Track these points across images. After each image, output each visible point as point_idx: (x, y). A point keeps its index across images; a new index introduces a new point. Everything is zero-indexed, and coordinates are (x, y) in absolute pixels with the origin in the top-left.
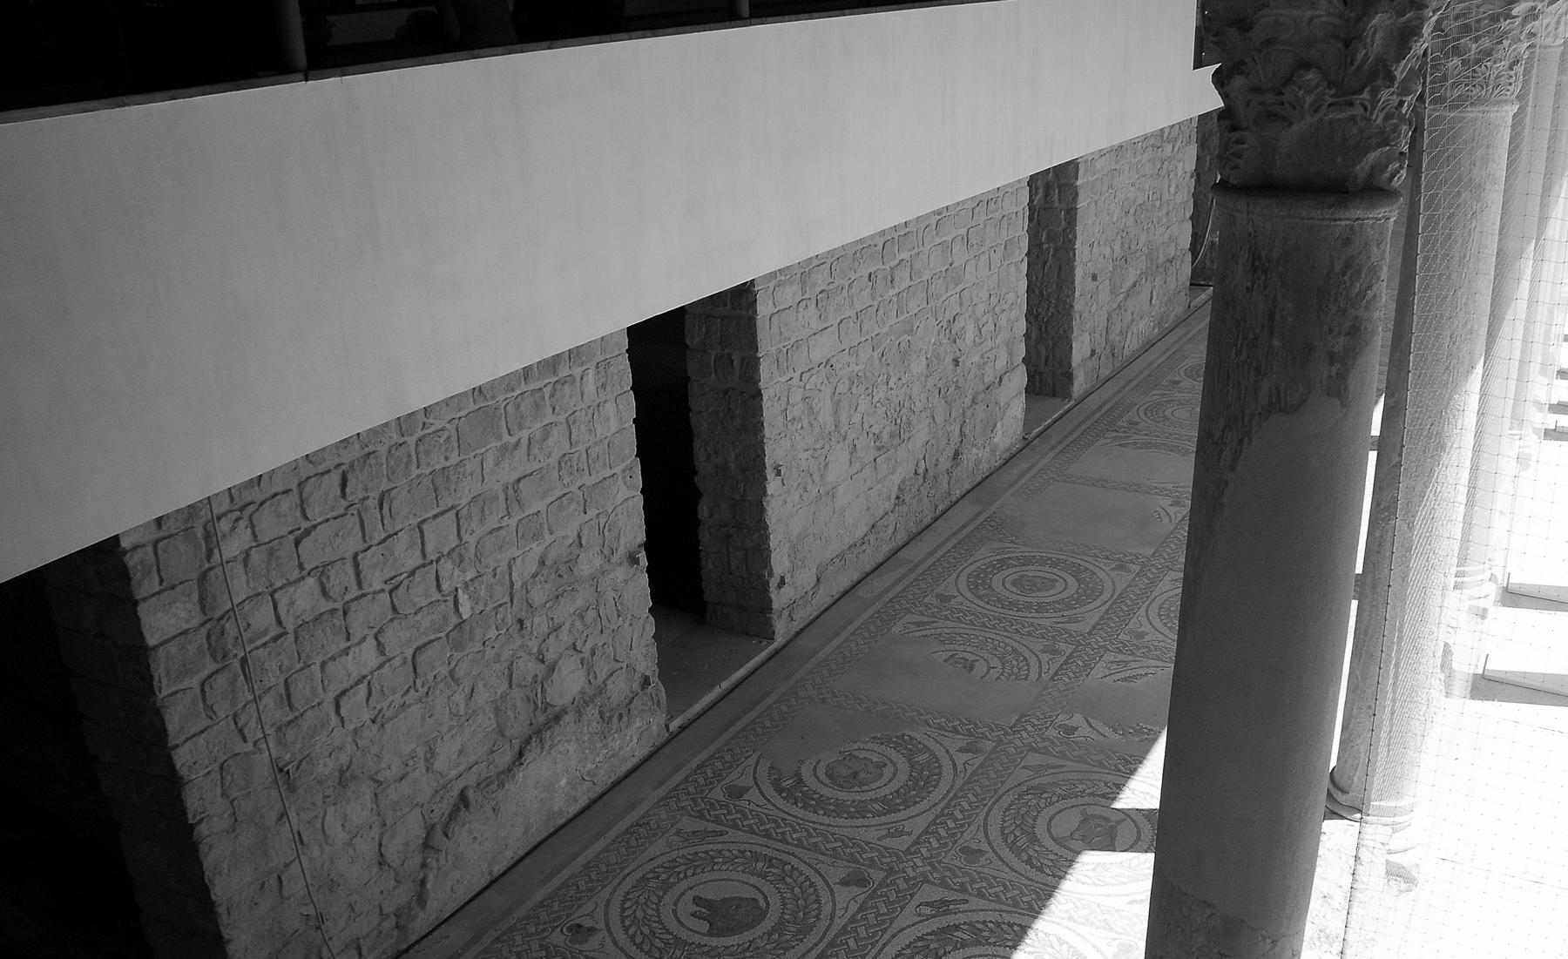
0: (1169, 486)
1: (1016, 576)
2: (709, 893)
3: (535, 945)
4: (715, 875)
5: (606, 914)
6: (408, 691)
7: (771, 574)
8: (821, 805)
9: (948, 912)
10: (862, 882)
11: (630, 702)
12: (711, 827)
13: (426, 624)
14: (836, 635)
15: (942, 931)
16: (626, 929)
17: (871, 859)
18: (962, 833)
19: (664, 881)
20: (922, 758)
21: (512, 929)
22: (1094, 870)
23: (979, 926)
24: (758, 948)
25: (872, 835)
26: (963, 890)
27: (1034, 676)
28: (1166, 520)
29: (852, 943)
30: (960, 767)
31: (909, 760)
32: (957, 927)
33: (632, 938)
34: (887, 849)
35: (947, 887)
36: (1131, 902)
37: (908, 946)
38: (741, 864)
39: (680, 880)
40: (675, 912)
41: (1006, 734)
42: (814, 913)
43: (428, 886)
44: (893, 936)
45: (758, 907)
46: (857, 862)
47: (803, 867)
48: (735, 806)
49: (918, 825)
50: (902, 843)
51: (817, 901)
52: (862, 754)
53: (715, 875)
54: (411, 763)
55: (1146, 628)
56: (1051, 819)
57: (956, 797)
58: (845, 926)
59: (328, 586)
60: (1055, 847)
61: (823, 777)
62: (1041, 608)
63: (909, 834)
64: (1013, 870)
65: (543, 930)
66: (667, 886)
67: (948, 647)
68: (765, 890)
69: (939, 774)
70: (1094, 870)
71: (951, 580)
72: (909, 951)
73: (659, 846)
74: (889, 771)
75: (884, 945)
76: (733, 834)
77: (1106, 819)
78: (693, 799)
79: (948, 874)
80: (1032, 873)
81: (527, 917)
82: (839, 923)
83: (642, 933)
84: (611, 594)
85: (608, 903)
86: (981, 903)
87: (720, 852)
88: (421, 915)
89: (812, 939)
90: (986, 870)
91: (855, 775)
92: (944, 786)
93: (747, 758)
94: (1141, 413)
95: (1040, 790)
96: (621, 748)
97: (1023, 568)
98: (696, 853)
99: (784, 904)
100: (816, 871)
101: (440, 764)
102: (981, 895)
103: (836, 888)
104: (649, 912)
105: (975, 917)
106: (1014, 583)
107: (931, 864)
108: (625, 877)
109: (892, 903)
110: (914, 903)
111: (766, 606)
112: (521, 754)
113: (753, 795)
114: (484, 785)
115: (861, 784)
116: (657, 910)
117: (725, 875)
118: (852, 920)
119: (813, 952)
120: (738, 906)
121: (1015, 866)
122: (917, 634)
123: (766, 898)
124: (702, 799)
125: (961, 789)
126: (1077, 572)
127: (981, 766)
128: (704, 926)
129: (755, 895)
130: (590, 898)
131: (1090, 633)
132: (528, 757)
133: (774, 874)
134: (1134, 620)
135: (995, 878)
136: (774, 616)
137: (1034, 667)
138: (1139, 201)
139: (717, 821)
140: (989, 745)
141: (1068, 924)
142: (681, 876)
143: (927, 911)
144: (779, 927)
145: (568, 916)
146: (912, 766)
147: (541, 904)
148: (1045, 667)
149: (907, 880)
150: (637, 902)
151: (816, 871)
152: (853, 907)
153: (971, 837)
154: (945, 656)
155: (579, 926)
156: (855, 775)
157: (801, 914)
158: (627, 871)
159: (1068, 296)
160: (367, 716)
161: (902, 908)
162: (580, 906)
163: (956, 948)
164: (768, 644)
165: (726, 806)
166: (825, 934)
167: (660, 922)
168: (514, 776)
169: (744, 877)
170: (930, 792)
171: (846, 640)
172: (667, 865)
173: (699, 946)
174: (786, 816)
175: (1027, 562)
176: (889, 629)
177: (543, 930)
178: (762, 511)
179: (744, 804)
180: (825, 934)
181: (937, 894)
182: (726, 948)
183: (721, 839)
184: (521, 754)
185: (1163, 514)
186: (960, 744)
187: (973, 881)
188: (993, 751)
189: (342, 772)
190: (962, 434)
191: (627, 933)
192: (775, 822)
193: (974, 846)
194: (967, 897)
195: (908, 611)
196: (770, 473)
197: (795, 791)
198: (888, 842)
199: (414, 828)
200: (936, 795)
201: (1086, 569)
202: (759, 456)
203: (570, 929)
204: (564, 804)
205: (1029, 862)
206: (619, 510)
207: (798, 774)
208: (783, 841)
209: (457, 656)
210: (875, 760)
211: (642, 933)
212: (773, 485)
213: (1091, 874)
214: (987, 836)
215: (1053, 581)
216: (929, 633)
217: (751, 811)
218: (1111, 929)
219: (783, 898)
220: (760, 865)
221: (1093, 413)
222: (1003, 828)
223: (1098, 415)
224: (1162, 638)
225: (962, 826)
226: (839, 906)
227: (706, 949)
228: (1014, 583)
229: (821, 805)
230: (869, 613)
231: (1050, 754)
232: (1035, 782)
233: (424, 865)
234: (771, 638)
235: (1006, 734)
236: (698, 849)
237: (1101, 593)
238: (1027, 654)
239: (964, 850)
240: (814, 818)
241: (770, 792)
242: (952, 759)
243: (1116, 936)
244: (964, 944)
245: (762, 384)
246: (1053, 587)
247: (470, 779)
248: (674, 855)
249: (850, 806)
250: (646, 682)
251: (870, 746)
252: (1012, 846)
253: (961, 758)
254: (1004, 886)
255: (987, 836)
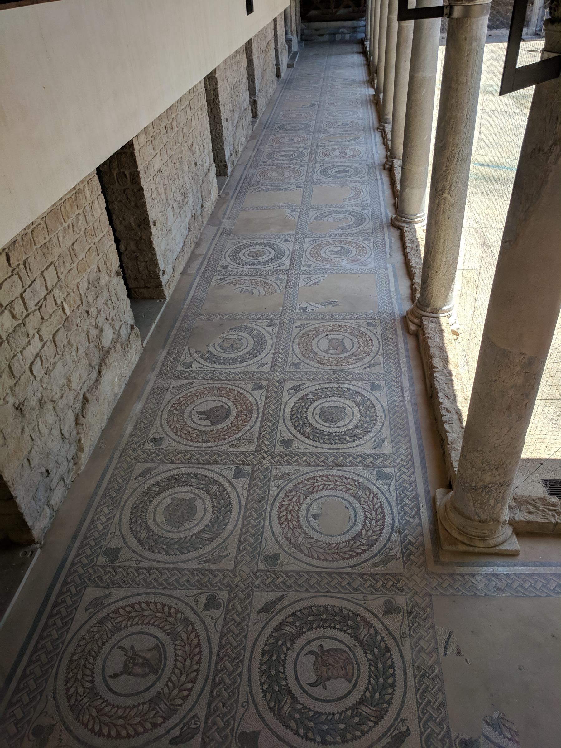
0: (287, 204)
1: (248, 252)
2: (202, 408)
3: (140, 452)
4: (200, 401)
5: (163, 430)
6: (55, 356)
7: (159, 270)
8: (225, 361)
9: (300, 390)
10: (261, 387)
11: (129, 338)
12: (186, 382)
13: (55, 322)
14: (189, 292)
15: (302, 398)
16: (176, 434)
17: (259, 377)
18: (287, 358)
19: (180, 409)
20: (255, 333)
21: (125, 449)
22: (344, 359)
23: (315, 392)
24: (235, 425)
25: (253, 368)
26: (301, 380)
27: (278, 291)
28: (293, 219)
29: (271, 412)
30: (271, 333)
31: (250, 335)
32: (307, 395)
33: (181, 436)
34: (262, 372)
35: (294, 380)
36: (365, 368)
37: (293, 407)
38: (208, 393)
39: (186, 407)
40: (192, 420)
41: (281, 316)
42: (249, 405)
43: (82, 442)
44: (286, 405)
45: (226, 409)
46: (253, 380)
47: (234, 388)
48: (191, 370)
49: (269, 359)
50: (267, 368)
51: (248, 400)
52: (230, 337)
53: (200, 401)
54: (63, 388)
55: (309, 263)
56: (317, 344)
57: (276, 345)
58: (264, 406)
59: (15, 313)
60: (324, 354)
61: (220, 350)
62: (265, 263)
63: (267, 363)
64: (315, 367)
65: (140, 445)
66: (182, 411)
67: (238, 286)
68: (224, 401)
69: (265, 337)
70: (344, 359)
71: (223, 259)
72: (294, 409)
73: (168, 396)
74: (244, 341)
75: (284, 409)
76: (197, 383)
77: (338, 339)
78: (171, 372)
79: (291, 375)
80: (322, 367)
81: (128, 442)
82: (261, 406)
83: (184, 434)
84: (113, 292)
85: (161, 425)
86: (310, 383)
87: (196, 391)
88: (83, 456)
89: (255, 415)
90: (305, 370)
91: (232, 346)
92: (269, 342)
93: (184, 350)
94: (258, 177)
95: (307, 334)
96: (131, 359)
97: (249, 248)
98: (186, 394)
99: (235, 405)
100: (240, 388)
101: (74, 385)
102: (308, 380)
103: (252, 392)
104: (182, 423)
105: (312, 389)
106: (249, 255)
107: (282, 373)
108: (162, 412)
109: (277, 392)
110: (285, 390)
111: (160, 285)
112: (100, 372)
113: (195, 364)
114: (90, 390)
115: (237, 349)
116: (185, 422)
117: (204, 399)
118: (266, 403)
119: (258, 420)
120: (217, 411)
121: (315, 366)
122: (222, 284)
123: (226, 404)
124: (175, 371)
125: (277, 341)
126: (271, 246)
127: (279, 330)
128: (209, 423)
129: (220, 404)
130: (152, 425)
131: (289, 269)
132: (103, 372)
133: (224, 394)
134: (303, 260)
135: (310, 372)
136: (164, 288)
137: (276, 287)
138: (234, 83)
139: (187, 378)
140: (277, 322)
141: (347, 382)
142: (186, 405)
143: (292, 391)
144: (239, 414)
145: (147, 435)
146: (253, 337)
147: (132, 434)
148: (280, 286)
149: (277, 382)
150: (174, 421)
151: (240, 388)
152: (263, 398)
153: (291, 359)
154: (239, 290)
155: (155, 439)
156: (232, 346)
157: (244, 406)
158: (161, 410)
159: (220, 130)
160: (43, 372)
161: (282, 393)
162: (150, 430)
163: (312, 403)
164: (164, 301)
165: (187, 372)
166: (258, 411)
167: (188, 426)
168: (100, 382)
169: (213, 398)
170: (265, 345)
171: (195, 292)
172: (177, 402)
173: (211, 431)
174: (214, 369)
175: (249, 246)
176: (210, 284)
177: (140, 445)
178: (151, 243)
179: (194, 369)
180: (258, 411)
181: (292, 384)
182: (223, 428)
183: (193, 385)
184: (100, 372)
185: (290, 216)
186: (266, 324)
187: (302, 376)
188: (280, 324)
189: (40, 401)
190: (202, 197)
191: (177, 435)
192: (211, 373)
193: (295, 362)
194: (304, 382)
195: (213, 275)
196: (151, 225)
197: (211, 358)
198: (261, 369)
199: (71, 418)
200: (269, 346)
201: (274, 244)
202: (146, 218)
203: (151, 441)
204: (119, 390)
205: (319, 362)
206: (109, 251)
207: (209, 351)
208: (219, 379)
209: (69, 333)
210: (236, 338)
211: (184, 434)
212: (153, 230)
213: (344, 361)
214: (297, 357)
215: (263, 251)
216: (227, 282)
217: (199, 371)
218: (364, 380)
219: (233, 402)
220: (216, 392)
221: (240, 180)
222: (302, 353)
223: (242, 181)
224: (318, 265)
225: (286, 355)
226: (257, 399)
227: (214, 432)
228: (249, 255)
229: (225, 361)
230: (198, 279)
231: (302, 320)
232: (303, 332)
233: (78, 433)
234: (164, 298)
235: (281, 316)
236: (187, 392)
237: (285, 252)
238: (270, 282)
239: (293, 364)
240: (226, 367)
241: (202, 361)
242: (266, 330)
243: (367, 382)
244: (313, 401)
245: (142, 184)
246: (265, 254)
247: (84, 390)
248: (177, 397)
249: (238, 358)
250: (132, 328)
251: (231, 333)
252: (309, 358)
253: (270, 329)
254: (315, 374)
255: (297, 357)
